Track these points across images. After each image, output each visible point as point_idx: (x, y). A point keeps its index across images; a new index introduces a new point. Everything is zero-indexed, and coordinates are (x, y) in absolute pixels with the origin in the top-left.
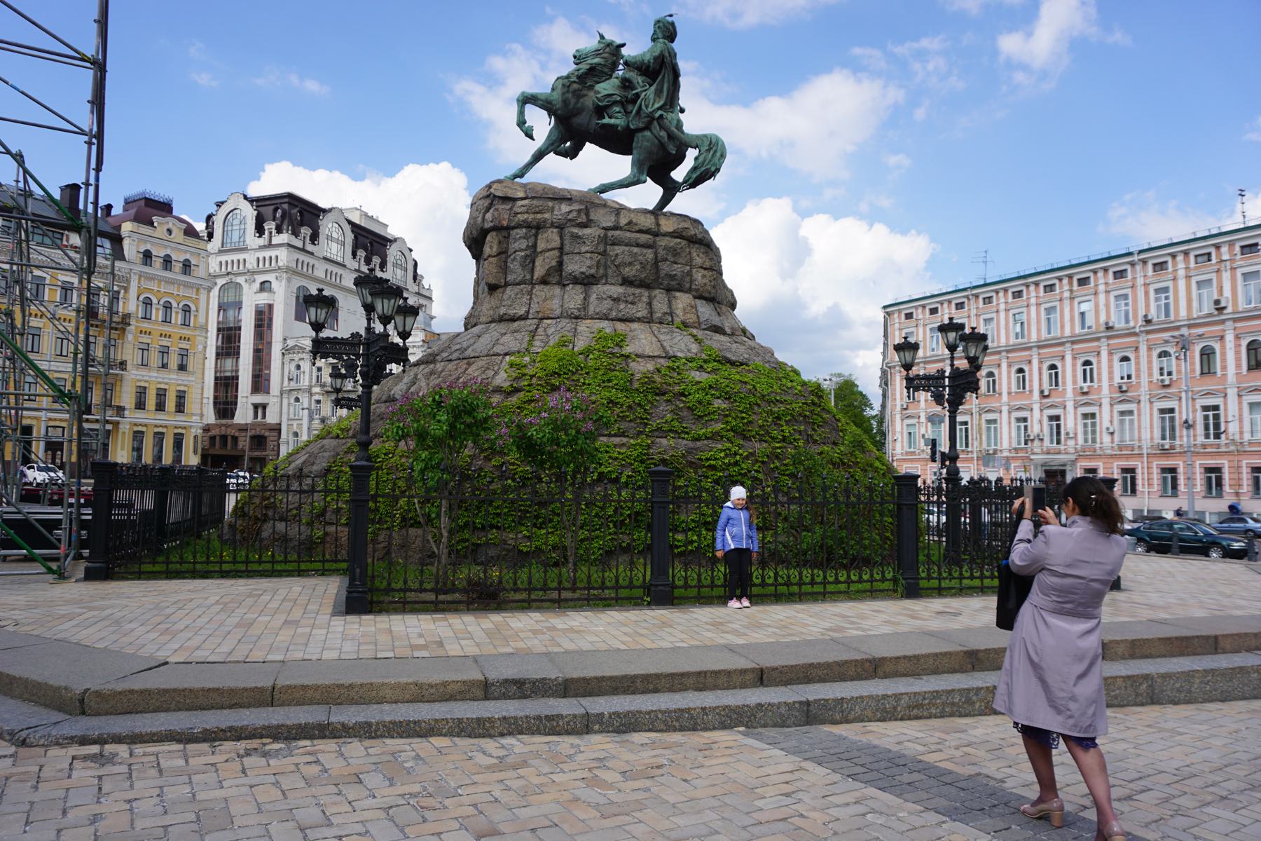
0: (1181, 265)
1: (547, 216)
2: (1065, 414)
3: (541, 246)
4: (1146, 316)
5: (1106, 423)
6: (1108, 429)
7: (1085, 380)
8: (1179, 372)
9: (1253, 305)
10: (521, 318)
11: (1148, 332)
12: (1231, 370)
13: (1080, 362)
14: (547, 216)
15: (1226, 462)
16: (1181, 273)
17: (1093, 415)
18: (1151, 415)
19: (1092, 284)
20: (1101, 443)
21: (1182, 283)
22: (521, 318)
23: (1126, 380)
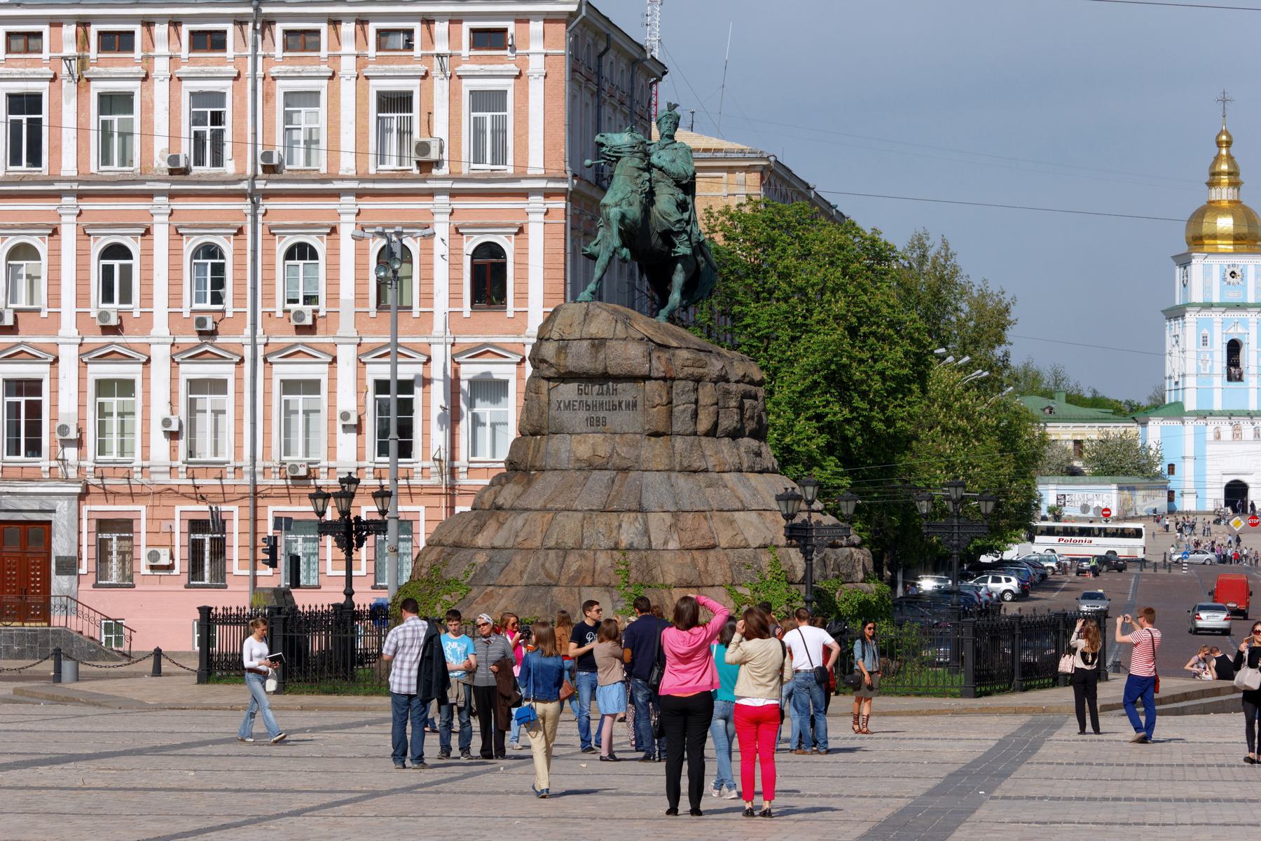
0: (348, 47)
1: (706, 370)
2: (55, 378)
3: (702, 402)
4: (268, 155)
5: (160, 409)
6: (166, 422)
7: (108, 297)
8: (333, 297)
9: (488, 166)
10: (706, 471)
11: (267, 195)
12: (441, 304)
13: (97, 247)
14: (706, 370)
15: (421, 509)
16: (348, 66)
17: (126, 387)
18: (268, 393)
19: (138, 53)
20: (145, 457)
21: (347, 89)
22: (706, 471)
23: (208, 305)
